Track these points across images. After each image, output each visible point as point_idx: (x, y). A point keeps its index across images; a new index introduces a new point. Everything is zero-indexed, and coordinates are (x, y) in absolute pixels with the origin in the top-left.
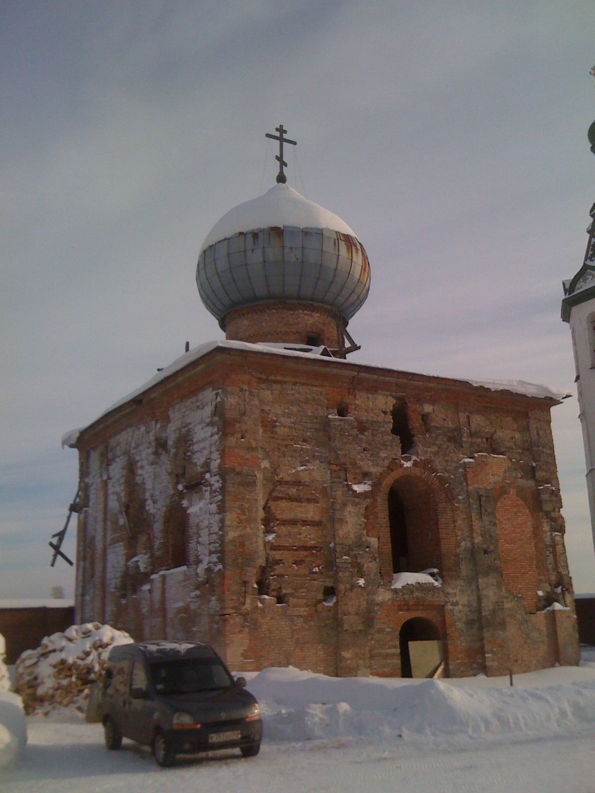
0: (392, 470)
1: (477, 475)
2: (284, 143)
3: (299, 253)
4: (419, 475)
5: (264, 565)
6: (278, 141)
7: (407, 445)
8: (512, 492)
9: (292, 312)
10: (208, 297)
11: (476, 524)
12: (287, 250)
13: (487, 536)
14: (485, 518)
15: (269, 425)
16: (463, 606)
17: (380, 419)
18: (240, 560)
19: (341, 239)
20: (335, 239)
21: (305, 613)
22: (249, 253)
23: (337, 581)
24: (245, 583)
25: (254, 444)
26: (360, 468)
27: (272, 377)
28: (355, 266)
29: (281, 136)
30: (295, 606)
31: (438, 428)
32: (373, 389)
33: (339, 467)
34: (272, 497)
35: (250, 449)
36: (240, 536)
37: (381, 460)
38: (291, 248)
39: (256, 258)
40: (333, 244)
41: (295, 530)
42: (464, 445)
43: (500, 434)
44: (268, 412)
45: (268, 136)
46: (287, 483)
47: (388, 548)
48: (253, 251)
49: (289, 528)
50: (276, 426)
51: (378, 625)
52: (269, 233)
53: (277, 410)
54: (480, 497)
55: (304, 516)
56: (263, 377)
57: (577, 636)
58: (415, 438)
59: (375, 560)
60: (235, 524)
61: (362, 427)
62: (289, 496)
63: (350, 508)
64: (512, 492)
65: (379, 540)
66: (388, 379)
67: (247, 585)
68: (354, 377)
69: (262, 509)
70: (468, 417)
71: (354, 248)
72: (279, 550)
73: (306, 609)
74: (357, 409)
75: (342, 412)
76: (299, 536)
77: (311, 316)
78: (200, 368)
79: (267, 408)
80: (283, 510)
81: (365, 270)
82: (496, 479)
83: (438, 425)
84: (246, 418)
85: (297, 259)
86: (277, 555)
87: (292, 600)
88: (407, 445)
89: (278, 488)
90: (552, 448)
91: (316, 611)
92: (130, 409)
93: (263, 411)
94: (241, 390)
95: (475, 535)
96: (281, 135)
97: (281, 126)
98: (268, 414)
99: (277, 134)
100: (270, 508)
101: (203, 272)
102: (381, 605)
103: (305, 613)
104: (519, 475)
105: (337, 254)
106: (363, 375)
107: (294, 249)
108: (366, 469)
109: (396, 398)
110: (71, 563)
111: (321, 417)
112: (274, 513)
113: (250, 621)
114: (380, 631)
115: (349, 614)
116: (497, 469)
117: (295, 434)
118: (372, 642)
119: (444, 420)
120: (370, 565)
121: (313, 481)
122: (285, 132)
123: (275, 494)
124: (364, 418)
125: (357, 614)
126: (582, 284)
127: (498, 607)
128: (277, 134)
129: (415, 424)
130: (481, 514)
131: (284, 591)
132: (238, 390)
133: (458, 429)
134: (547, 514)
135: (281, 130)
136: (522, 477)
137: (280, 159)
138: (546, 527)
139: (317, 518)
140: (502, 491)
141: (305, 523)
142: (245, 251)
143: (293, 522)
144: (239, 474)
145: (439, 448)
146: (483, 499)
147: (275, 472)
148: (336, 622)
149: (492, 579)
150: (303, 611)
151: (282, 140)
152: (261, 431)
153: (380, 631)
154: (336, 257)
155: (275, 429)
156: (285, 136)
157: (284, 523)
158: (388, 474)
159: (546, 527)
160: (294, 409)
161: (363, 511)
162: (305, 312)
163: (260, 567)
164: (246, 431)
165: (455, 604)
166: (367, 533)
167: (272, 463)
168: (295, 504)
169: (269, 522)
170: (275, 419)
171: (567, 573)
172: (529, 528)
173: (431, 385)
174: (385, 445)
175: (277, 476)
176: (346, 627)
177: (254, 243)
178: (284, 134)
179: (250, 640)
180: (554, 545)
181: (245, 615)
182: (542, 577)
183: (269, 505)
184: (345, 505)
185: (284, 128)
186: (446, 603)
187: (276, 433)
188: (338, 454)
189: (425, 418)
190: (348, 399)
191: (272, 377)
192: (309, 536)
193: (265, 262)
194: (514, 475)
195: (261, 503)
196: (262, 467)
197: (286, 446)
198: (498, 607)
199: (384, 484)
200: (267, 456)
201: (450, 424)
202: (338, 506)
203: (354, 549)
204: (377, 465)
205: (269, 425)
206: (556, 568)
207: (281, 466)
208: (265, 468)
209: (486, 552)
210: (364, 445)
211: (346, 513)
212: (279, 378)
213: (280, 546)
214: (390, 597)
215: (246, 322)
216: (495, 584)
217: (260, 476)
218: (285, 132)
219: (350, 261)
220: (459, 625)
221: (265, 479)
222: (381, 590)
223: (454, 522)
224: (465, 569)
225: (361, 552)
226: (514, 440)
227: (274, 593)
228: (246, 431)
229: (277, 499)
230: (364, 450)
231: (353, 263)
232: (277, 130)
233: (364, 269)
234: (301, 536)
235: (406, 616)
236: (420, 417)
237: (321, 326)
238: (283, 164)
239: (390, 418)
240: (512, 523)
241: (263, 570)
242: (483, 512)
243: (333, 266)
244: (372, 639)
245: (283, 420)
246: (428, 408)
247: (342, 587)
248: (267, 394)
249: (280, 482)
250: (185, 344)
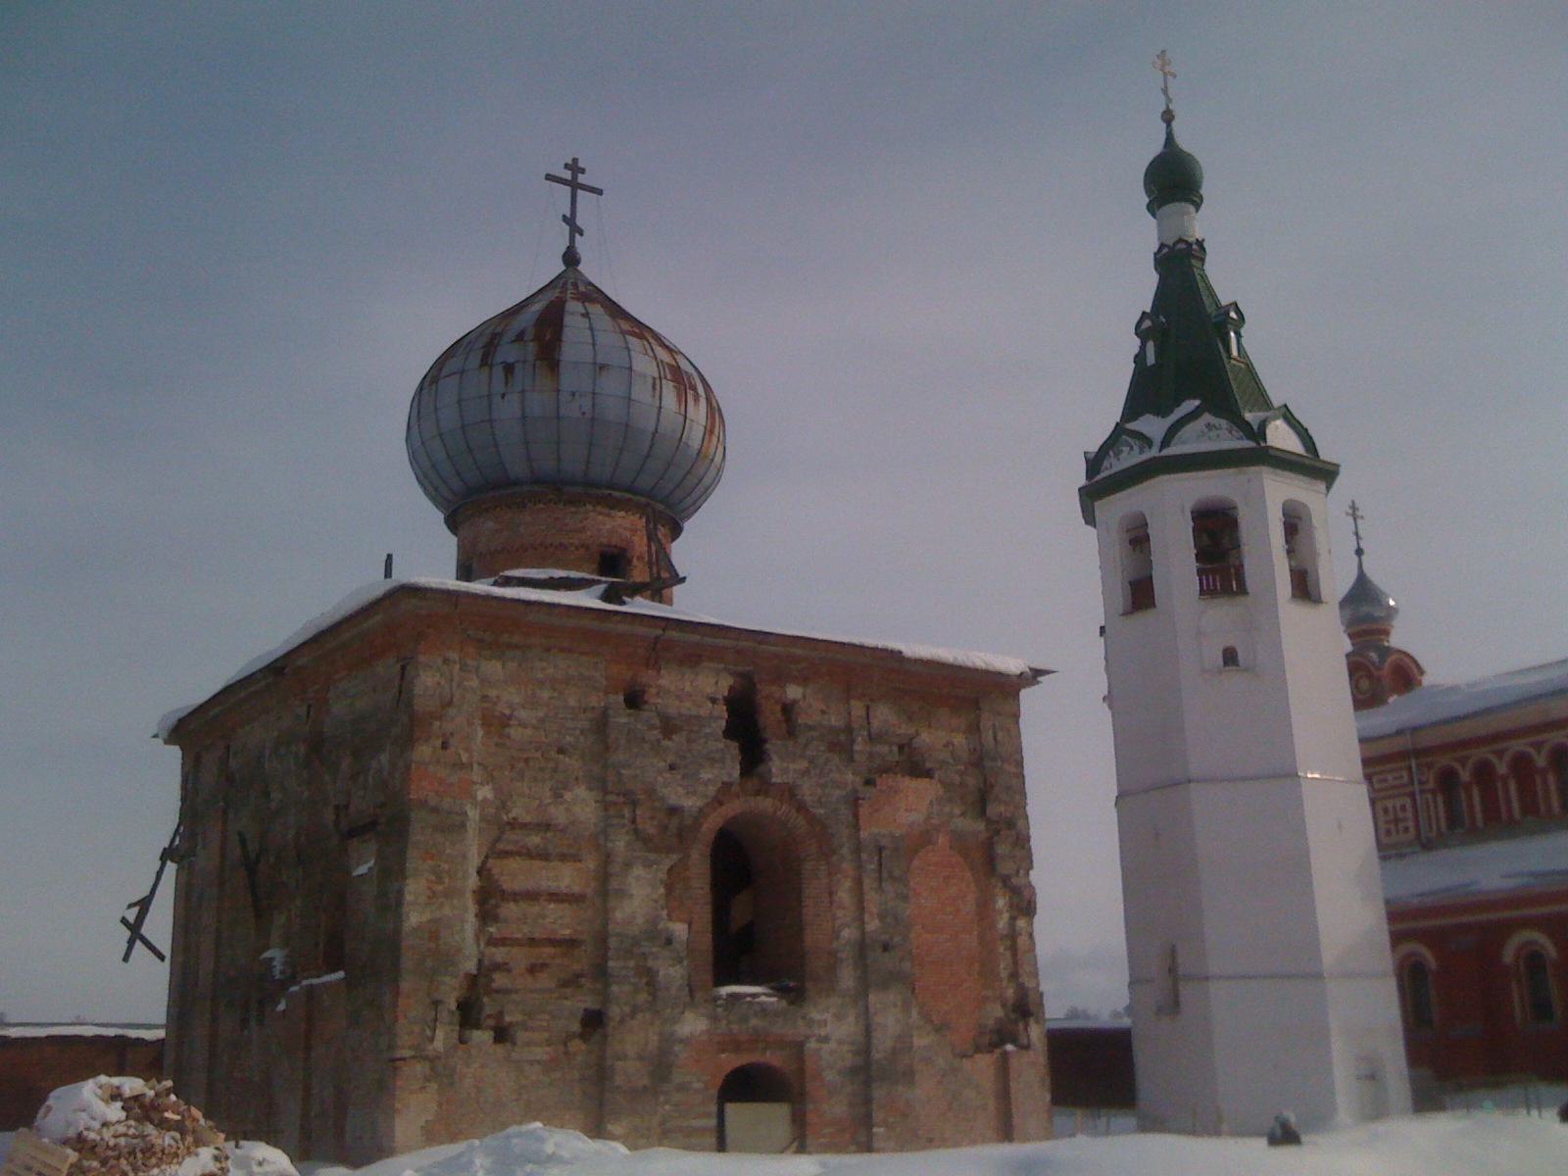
0: (721, 804)
1: (877, 811)
2: (580, 192)
3: (587, 403)
4: (771, 810)
5: (475, 972)
6: (568, 189)
7: (753, 755)
8: (942, 840)
9: (573, 509)
10: (426, 477)
11: (872, 897)
12: (564, 397)
13: (889, 920)
14: (887, 886)
15: (497, 723)
16: (840, 1042)
17: (703, 712)
18: (429, 963)
19: (665, 378)
20: (654, 379)
21: (545, 1057)
22: (497, 399)
23: (606, 999)
24: (436, 1004)
25: (465, 758)
26: (662, 799)
27: (505, 638)
28: (691, 428)
29: (573, 178)
30: (528, 1044)
31: (811, 728)
32: (692, 659)
33: (622, 799)
34: (495, 852)
35: (459, 766)
36: (430, 921)
37: (700, 784)
38: (573, 394)
39: (508, 410)
40: (650, 387)
41: (536, 909)
42: (857, 757)
43: (925, 738)
44: (495, 699)
45: (549, 177)
46: (524, 826)
47: (706, 941)
48: (503, 396)
49: (523, 905)
50: (508, 726)
51: (678, 1077)
52: (534, 366)
53: (510, 697)
54: (880, 850)
55: (553, 886)
57: (1048, 1097)
58: (768, 746)
59: (680, 962)
60: (423, 899)
61: (669, 727)
62: (528, 849)
63: (638, 871)
64: (942, 840)
65: (689, 927)
66: (720, 642)
67: (439, 1008)
68: (657, 638)
69: (475, 874)
70: (868, 708)
71: (690, 393)
72: (504, 945)
73: (548, 1049)
74: (661, 694)
75: (634, 700)
76: (541, 921)
77: (608, 515)
78: (378, 618)
79: (493, 693)
80: (515, 874)
81: (712, 432)
82: (913, 817)
83: (810, 723)
84: (452, 711)
85: (584, 413)
86: (499, 954)
87: (521, 1036)
88: (753, 755)
89: (510, 836)
90: (1020, 764)
91: (566, 1053)
92: (263, 683)
93: (485, 698)
94: (446, 661)
95: (867, 917)
96: (574, 177)
97: (575, 160)
98: (495, 704)
99: (567, 175)
100: (489, 870)
101: (415, 430)
102: (686, 1041)
104: (957, 811)
105: (658, 405)
106: (673, 634)
107: (577, 397)
108: (673, 801)
109: (733, 674)
110: (162, 958)
111: (593, 708)
112: (497, 881)
113: (441, 1072)
114: (682, 1088)
115: (624, 1057)
116: (912, 804)
117: (543, 739)
118: (667, 1107)
119: (823, 712)
120: (671, 970)
121: (573, 823)
122: (583, 171)
123: (500, 846)
124: (672, 711)
125: (640, 1058)
126: (1113, 460)
127: (903, 1045)
128: (567, 175)
129: (769, 717)
130: (880, 879)
131: (507, 1019)
132: (440, 661)
133: (849, 729)
134: (1005, 880)
135: (574, 167)
136: (963, 814)
137: (570, 221)
138: (1001, 903)
139: (576, 889)
140: (923, 839)
141: (555, 897)
142: (489, 395)
143: (532, 896)
144: (435, 810)
145: (811, 762)
147: (503, 806)
148: (600, 1076)
149: (893, 996)
150: (541, 1053)
151: (575, 186)
152: (480, 733)
153: (682, 1088)
154: (656, 410)
155: (507, 730)
156: (581, 179)
157: (516, 897)
158: (715, 809)
159: (1001, 903)
160: (545, 694)
161: (662, 875)
162: (599, 508)
163: (468, 975)
164: (452, 734)
165: (826, 1039)
166: (668, 915)
167: (498, 791)
168: (538, 863)
169: (489, 898)
170: (507, 712)
171: (1034, 985)
172: (969, 906)
173: (798, 651)
174: (713, 761)
175: (507, 814)
176: (619, 1080)
177: (506, 383)
178: (580, 175)
179: (440, 1105)
180: (1012, 936)
181: (432, 1060)
182: (990, 993)
183: (488, 865)
184: (628, 865)
185: (581, 164)
186: (808, 1037)
187: (509, 736)
188: (620, 775)
189: (788, 709)
190: (646, 676)
191: (505, 638)
192: (559, 920)
193: (524, 417)
194: (947, 809)
195: (474, 861)
196: (480, 797)
197: (527, 760)
198: (903, 1045)
199: (704, 828)
200: (490, 778)
201: (835, 720)
202: (615, 868)
203: (643, 943)
204: (694, 793)
205: (497, 723)
206: (1014, 976)
207: (515, 797)
208: (485, 800)
209: (886, 948)
210: (671, 758)
211: (631, 880)
212: (516, 639)
214: (704, 1028)
215: (490, 524)
216: (899, 1003)
217: (473, 814)
218: (583, 171)
219: (682, 419)
220: (830, 1076)
221: (483, 818)
222: (689, 1015)
223: (831, 894)
224: (847, 978)
225: (654, 950)
226: (951, 747)
227: (491, 1022)
228: (452, 734)
229: (507, 854)
230: (672, 767)
231: (688, 421)
232: (566, 166)
233: (709, 431)
234: (548, 920)
235: (731, 1061)
236: (779, 708)
238: (575, 230)
239: (722, 710)
240: (937, 897)
241: (473, 981)
242: (885, 875)
243: (652, 429)
244: (667, 1102)
245: (523, 714)
246: (793, 692)
247: (615, 1011)
248: (493, 668)
249: (513, 825)
250: (385, 558)
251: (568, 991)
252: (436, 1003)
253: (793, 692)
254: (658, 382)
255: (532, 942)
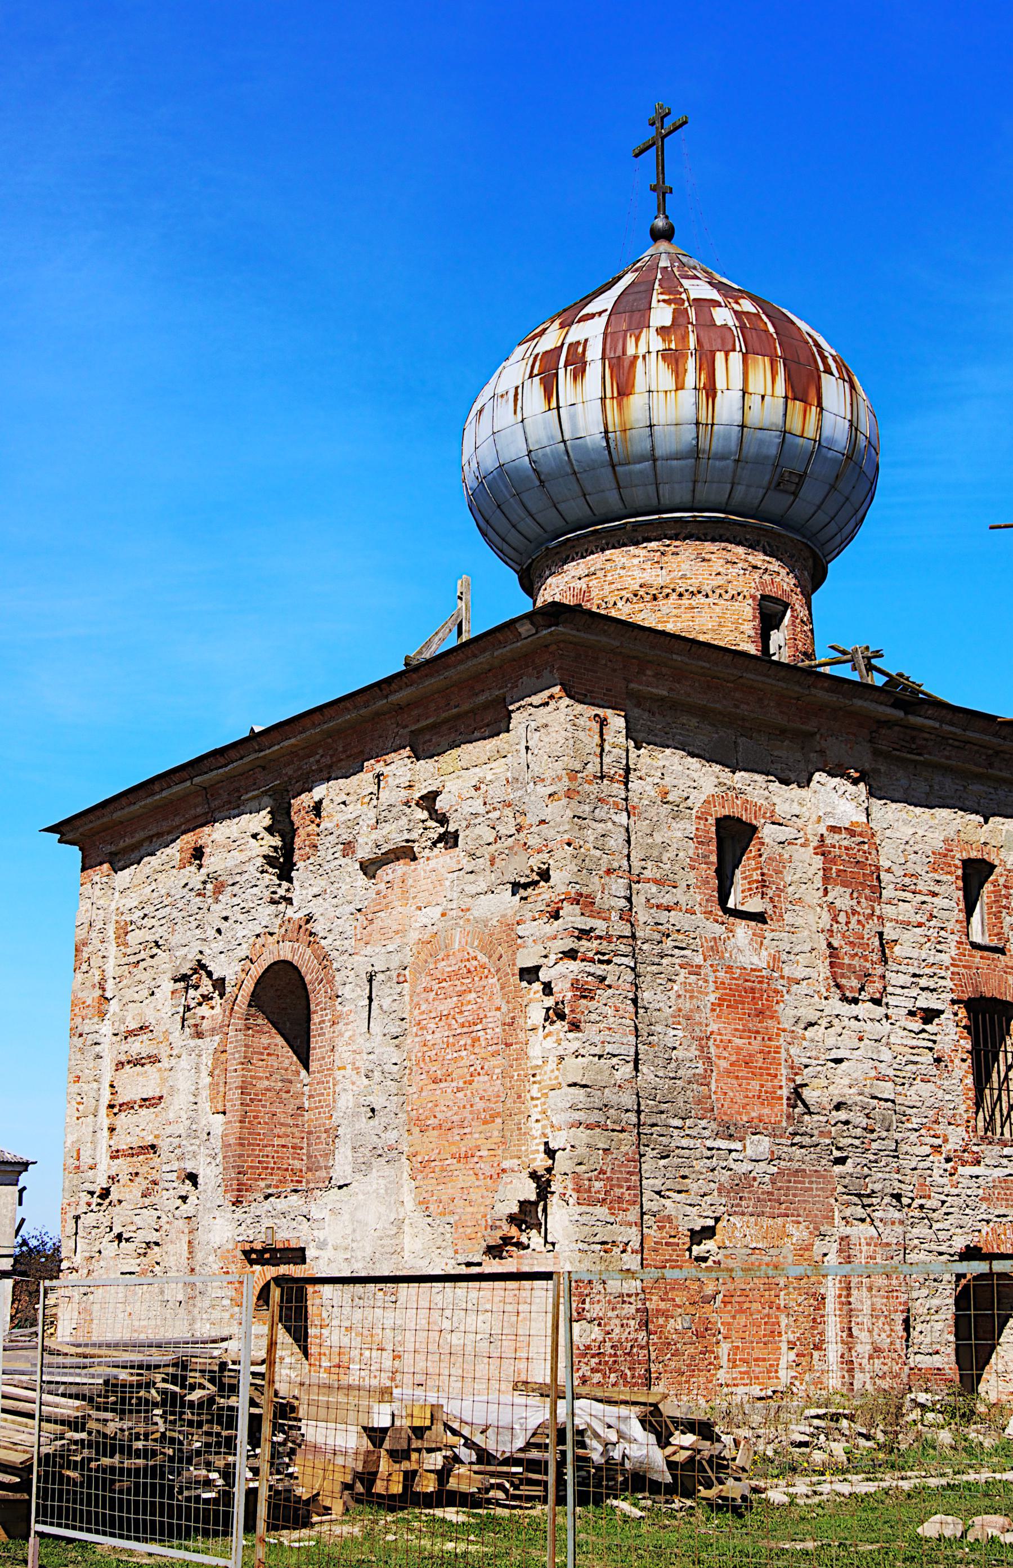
4: (289, 958)
28: (573, 418)
56: (113, 849)
103: (138, 1269)
146: (380, 977)
159: (536, 1015)
187: (126, 945)
212: (128, 841)
213: (117, 1151)
237: (582, 584)
249: (130, 1034)
251: (147, 1201)
252: (77, 1218)
253: (319, 792)
254: (520, 390)
255: (132, 1153)
